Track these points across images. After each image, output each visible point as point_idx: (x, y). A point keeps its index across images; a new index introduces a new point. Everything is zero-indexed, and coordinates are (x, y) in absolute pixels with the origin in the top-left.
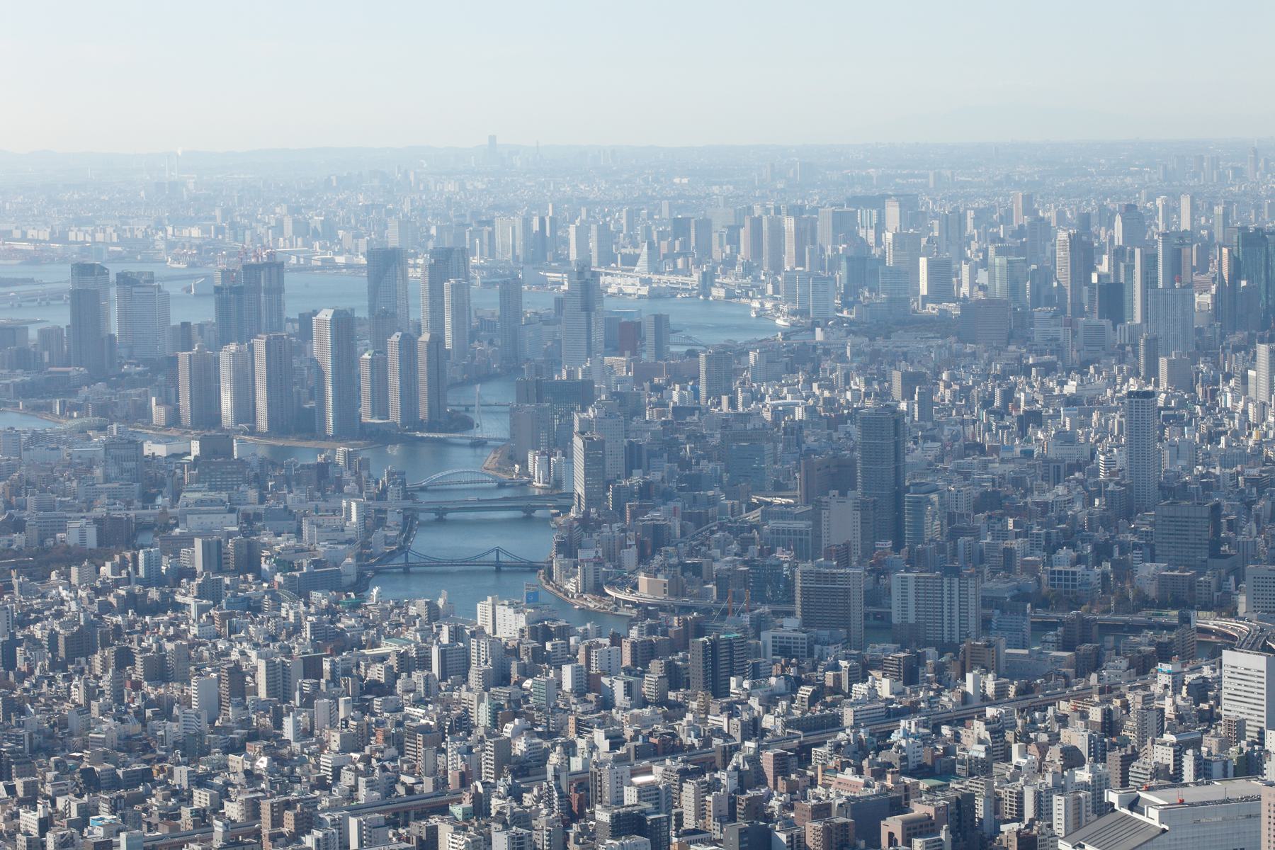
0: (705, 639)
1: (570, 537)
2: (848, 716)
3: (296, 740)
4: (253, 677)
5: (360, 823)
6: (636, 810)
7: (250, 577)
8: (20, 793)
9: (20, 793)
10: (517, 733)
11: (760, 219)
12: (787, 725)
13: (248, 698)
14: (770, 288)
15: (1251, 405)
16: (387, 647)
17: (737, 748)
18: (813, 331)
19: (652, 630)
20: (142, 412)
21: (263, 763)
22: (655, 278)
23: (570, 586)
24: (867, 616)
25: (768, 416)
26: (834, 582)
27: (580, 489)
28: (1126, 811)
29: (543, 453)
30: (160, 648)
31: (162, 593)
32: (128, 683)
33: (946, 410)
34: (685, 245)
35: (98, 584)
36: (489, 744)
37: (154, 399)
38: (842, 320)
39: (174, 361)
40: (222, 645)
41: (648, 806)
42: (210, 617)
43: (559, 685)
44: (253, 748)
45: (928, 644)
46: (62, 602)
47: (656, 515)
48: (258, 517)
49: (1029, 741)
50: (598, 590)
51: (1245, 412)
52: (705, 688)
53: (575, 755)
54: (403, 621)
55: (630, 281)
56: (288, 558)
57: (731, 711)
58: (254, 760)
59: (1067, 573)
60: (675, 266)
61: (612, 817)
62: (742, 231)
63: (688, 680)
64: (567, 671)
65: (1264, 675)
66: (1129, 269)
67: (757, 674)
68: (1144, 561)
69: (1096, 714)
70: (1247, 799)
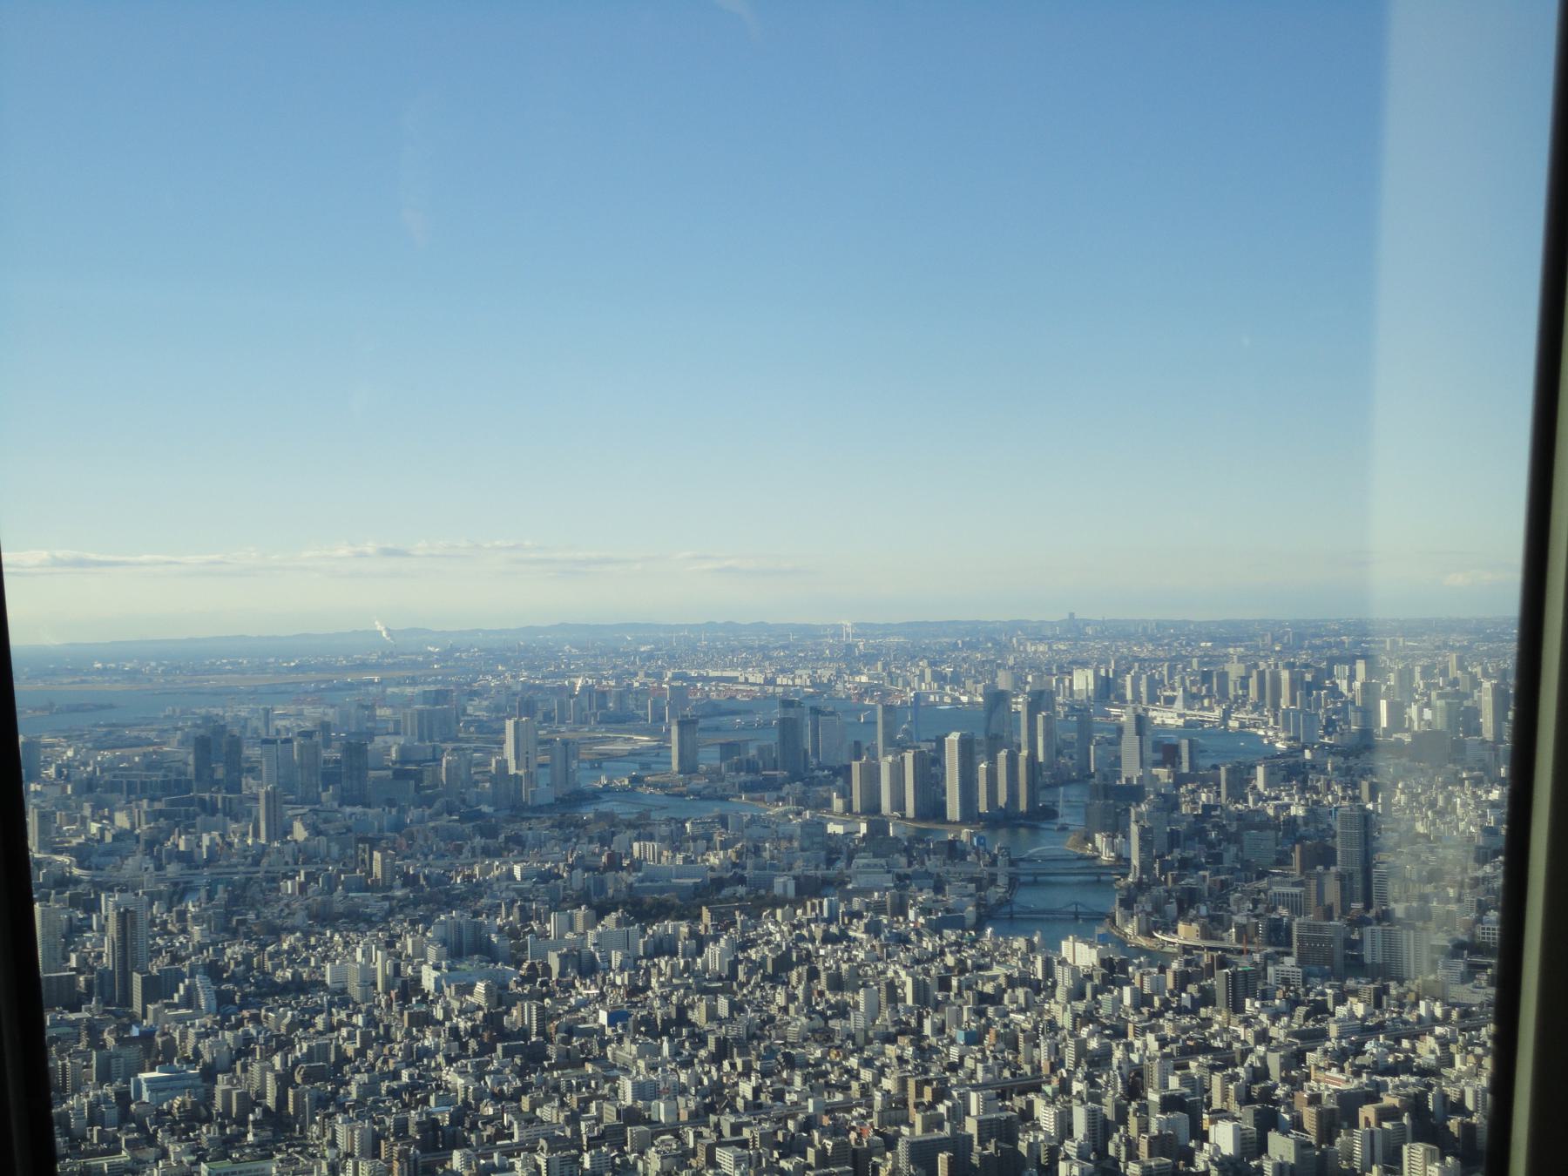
0: (1227, 970)
2: (1333, 1030)
6: (1177, 1093)
7: (901, 919)
8: (740, 1068)
9: (740, 1068)
10: (1091, 1035)
11: (1264, 671)
12: (1287, 1035)
13: (900, 1006)
14: (1271, 720)
16: (997, 970)
17: (1251, 1051)
18: (1303, 752)
19: (1188, 963)
20: (828, 803)
21: (909, 1051)
23: (1128, 930)
24: (1346, 956)
25: (1271, 812)
26: (1320, 932)
27: (1135, 862)
29: (1109, 836)
30: (838, 968)
31: (840, 930)
32: (816, 992)
33: (1402, 810)
34: (1209, 690)
35: (795, 922)
36: (1071, 1042)
38: (1324, 744)
39: (849, 768)
40: (881, 966)
41: (1187, 1090)
42: (873, 946)
43: (1121, 1001)
44: (903, 1041)
45: (1392, 979)
46: (771, 934)
47: (1189, 881)
48: (907, 877)
49: (1468, 1053)
50: (1148, 934)
52: (1228, 1006)
53: (1133, 1052)
54: (1009, 952)
55: (1170, 715)
56: (928, 906)
57: (1247, 1022)
58: (903, 1049)
60: (1203, 704)
62: (1251, 680)
64: (1127, 991)
67: (1265, 996)
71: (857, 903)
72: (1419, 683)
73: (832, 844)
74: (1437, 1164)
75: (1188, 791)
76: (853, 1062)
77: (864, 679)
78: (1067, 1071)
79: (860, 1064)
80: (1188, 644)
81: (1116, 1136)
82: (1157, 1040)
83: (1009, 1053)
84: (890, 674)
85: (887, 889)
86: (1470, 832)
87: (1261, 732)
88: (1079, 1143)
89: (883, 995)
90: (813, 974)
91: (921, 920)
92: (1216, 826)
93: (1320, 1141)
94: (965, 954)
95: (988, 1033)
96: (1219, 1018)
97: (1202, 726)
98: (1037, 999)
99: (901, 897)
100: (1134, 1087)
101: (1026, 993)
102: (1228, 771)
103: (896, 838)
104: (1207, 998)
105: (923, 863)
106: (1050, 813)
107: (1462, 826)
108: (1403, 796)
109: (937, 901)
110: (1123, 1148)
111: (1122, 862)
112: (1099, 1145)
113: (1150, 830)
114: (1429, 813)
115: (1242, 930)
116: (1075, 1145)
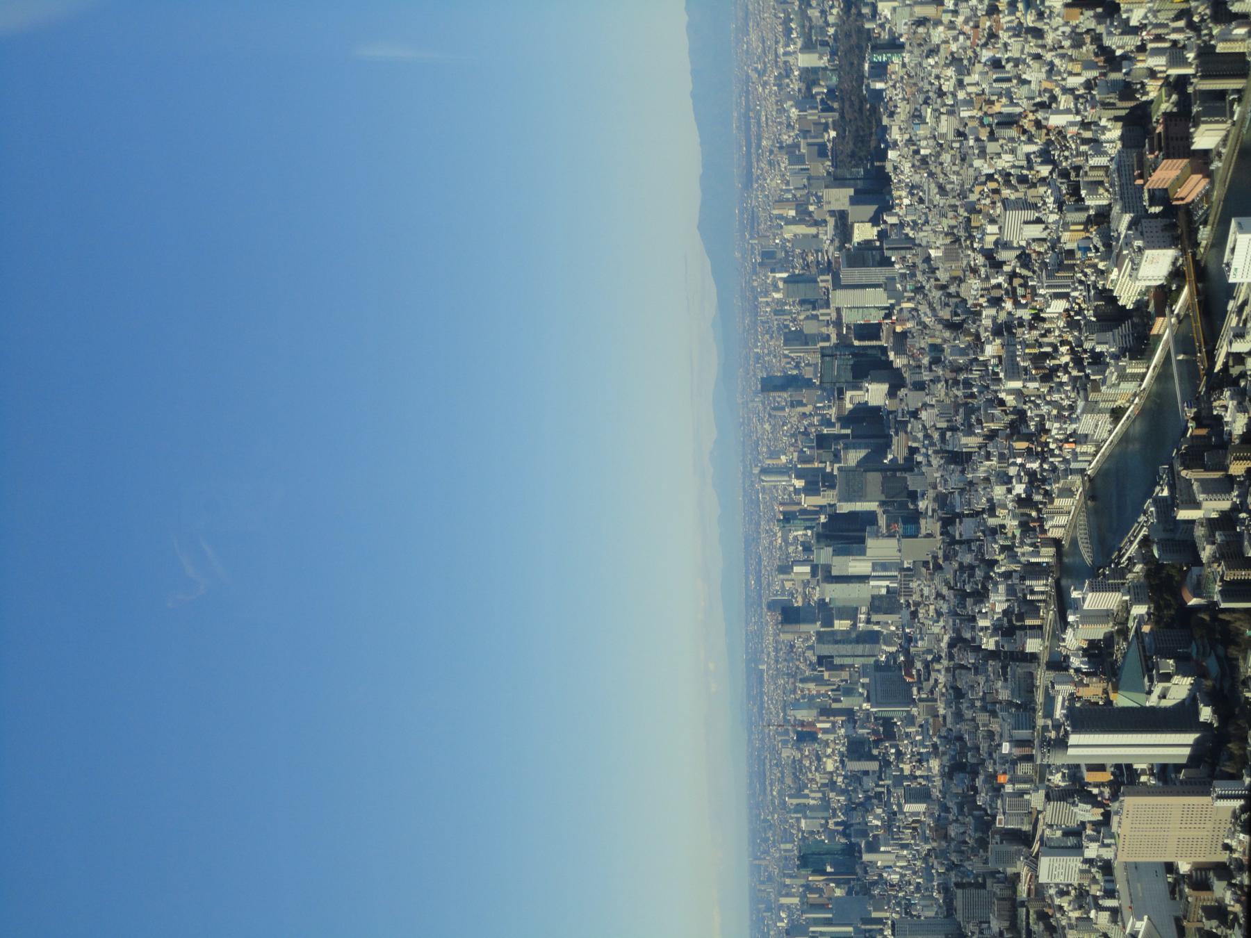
15: (898, 864)
51: (901, 867)
65: (1052, 858)
70: (1126, 869)
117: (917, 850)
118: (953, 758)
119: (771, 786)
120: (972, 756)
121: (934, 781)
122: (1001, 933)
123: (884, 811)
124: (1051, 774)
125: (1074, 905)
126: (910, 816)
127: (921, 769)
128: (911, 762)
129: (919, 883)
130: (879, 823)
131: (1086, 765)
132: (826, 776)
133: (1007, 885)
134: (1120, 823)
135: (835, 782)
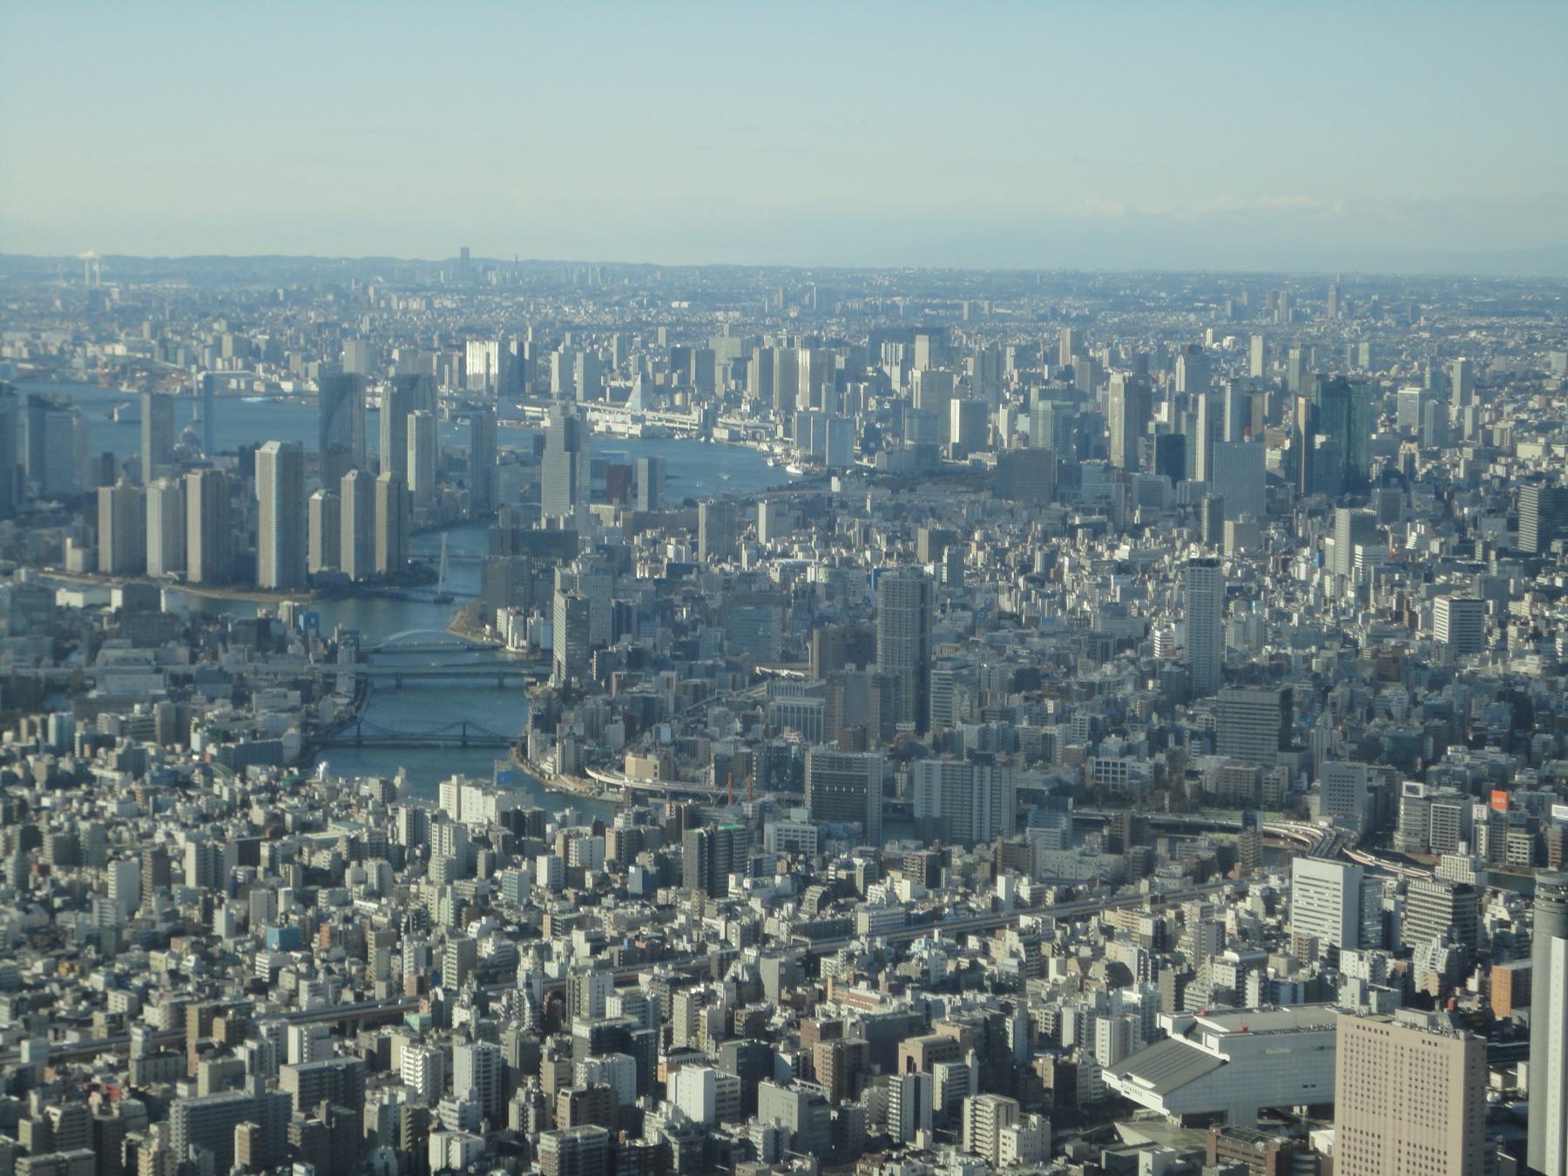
0: (701, 830)
1: (548, 710)
2: (863, 922)
3: (229, 935)
4: (180, 862)
5: (301, 1034)
7: (178, 747)
10: (484, 933)
11: (771, 349)
12: (794, 930)
13: (176, 889)
14: (780, 429)
15: (1328, 579)
16: (334, 831)
17: (736, 956)
18: (829, 481)
19: (640, 818)
20: (57, 555)
21: (190, 961)
22: (649, 415)
23: (547, 766)
24: (886, 807)
25: (775, 576)
26: (849, 768)
27: (560, 655)
28: (1179, 1038)
29: (518, 613)
30: (73, 828)
31: (78, 767)
34: (684, 379)
36: (452, 946)
37: (69, 541)
38: (861, 469)
39: (93, 498)
40: (144, 825)
41: (634, 1020)
42: (131, 793)
43: (533, 879)
44: (180, 945)
45: (953, 842)
47: (646, 686)
48: (188, 679)
49: (1069, 955)
51: (1321, 585)
52: (701, 885)
53: (550, 959)
54: (353, 801)
55: (620, 418)
57: (729, 912)
58: (179, 958)
59: (1115, 765)
60: (672, 402)
61: (592, 1032)
62: (749, 365)
63: (681, 876)
64: (542, 863)
66: (1193, 418)
67: (758, 870)
68: (1203, 752)
69: (1146, 927)
70: (1320, 1028)
71: (105, 723)
72: (1011, 371)
73: (65, 624)
74: (1016, 1127)
75: (645, 541)
76: (96, 981)
77: (120, 350)
78: (446, 991)
79: (108, 984)
80: (652, 304)
81: (521, 1093)
82: (587, 940)
83: (352, 963)
84: (163, 342)
85: (156, 699)
86: (1083, 612)
87: (764, 447)
88: (462, 1104)
89: (147, 872)
90: (31, 839)
91: (212, 750)
92: (693, 599)
93: (838, 1092)
94: (281, 805)
95: (318, 931)
96: (687, 905)
97: (671, 437)
98: (399, 877)
99: (179, 712)
100: (551, 1019)
101: (380, 868)
102: (710, 509)
103: (172, 616)
104: (668, 874)
105: (215, 656)
106: (424, 575)
107: (1070, 601)
108: (981, 554)
109: (238, 719)
110: (532, 1112)
111: (540, 655)
112: (493, 1103)
113: (585, 604)
114: (1021, 581)
115: (725, 768)
116: (456, 1106)
117: (1355, 618)
118: (1543, 705)
119: (1488, 328)
120: (1545, 744)
121: (1495, 662)
122: (1193, 774)
123: (1434, 556)
124: (1508, 900)
125: (1248, 921)
126: (1424, 609)
127: (1521, 633)
128: (1535, 618)
129: (1290, 619)
130: (1410, 545)
131: (1528, 972)
132: (1507, 443)
133: (1286, 793)
134: (1413, 1026)
135: (1494, 461)
